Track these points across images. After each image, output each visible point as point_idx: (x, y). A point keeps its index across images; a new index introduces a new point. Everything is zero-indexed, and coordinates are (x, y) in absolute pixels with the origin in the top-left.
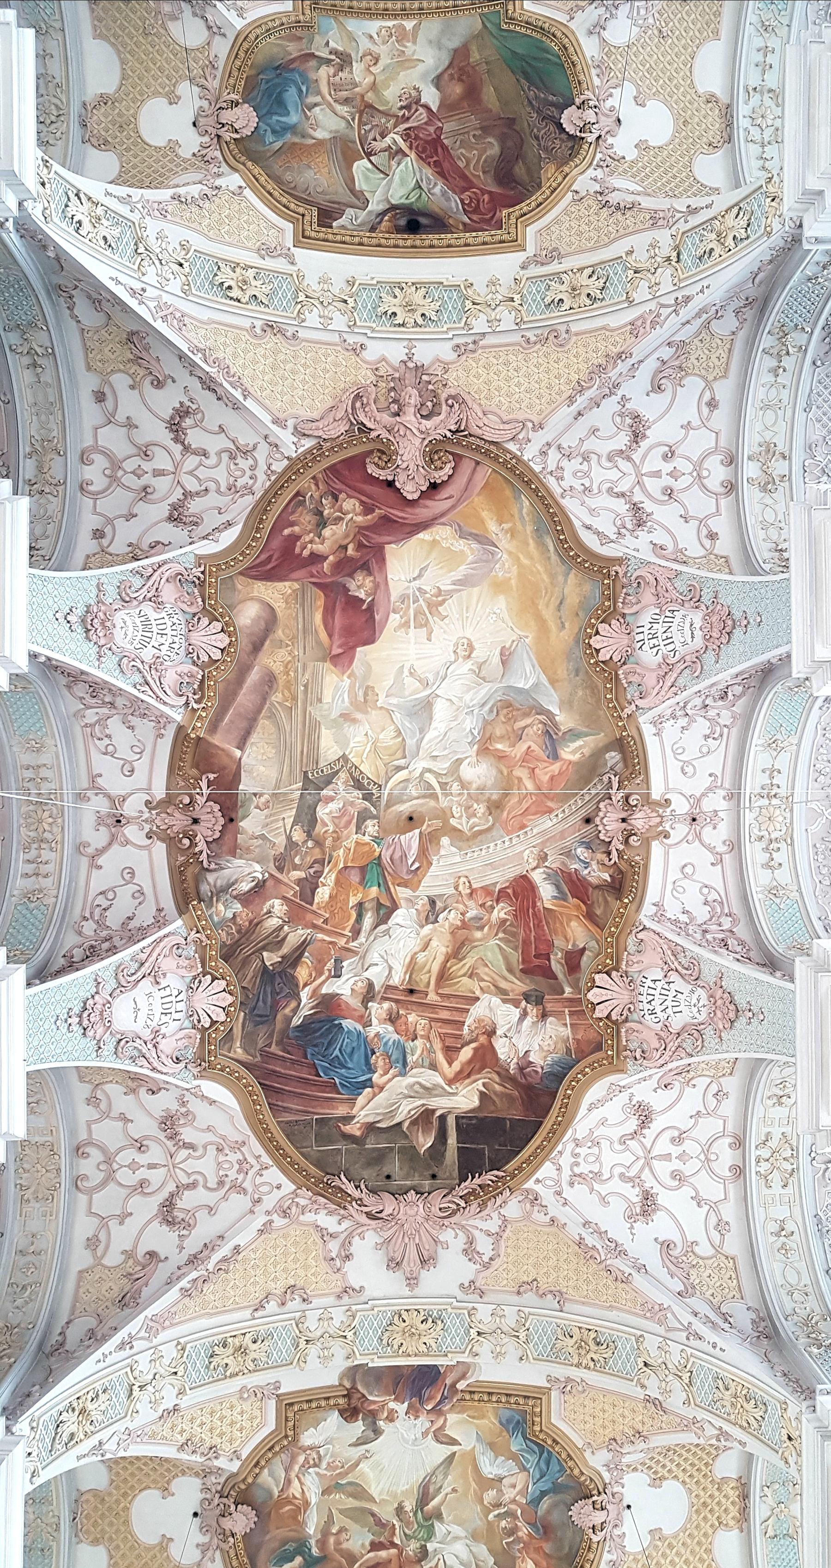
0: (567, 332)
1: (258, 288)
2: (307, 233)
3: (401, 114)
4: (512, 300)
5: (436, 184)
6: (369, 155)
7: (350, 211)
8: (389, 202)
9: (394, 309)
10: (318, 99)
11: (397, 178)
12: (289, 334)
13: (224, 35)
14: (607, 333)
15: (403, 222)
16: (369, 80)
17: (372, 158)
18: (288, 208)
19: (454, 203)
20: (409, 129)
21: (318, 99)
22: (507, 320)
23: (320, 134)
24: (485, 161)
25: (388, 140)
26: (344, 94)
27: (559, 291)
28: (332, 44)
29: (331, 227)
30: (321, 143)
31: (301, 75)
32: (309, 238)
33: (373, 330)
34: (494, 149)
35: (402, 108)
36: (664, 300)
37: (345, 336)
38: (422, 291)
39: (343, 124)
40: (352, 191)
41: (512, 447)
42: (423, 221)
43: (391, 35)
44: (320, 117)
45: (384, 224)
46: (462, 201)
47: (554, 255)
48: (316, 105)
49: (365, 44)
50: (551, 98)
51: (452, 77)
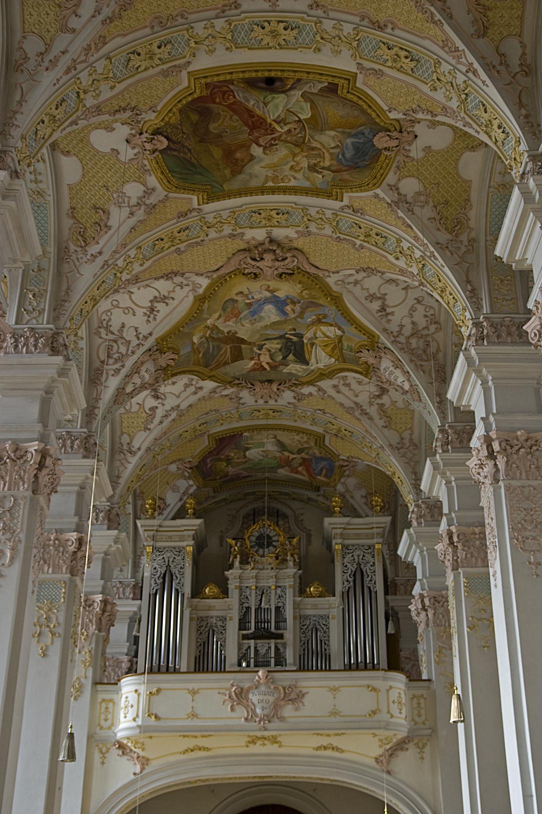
0: (153, 27)
1: (387, 54)
2: (347, 82)
3: (277, 142)
4: (196, 43)
5: (254, 105)
6: (300, 121)
7: (315, 90)
8: (287, 95)
9: (285, 32)
10: (332, 151)
11: (281, 108)
12: (367, 20)
13: (389, 185)
14: (122, 32)
15: (277, 84)
16: (297, 159)
17: (297, 119)
18: (358, 97)
19: (240, 96)
20: (271, 134)
21: (332, 151)
23: (332, 133)
24: (219, 120)
25: (286, 128)
27: (164, 52)
28: (320, 176)
29: (329, 83)
30: (332, 129)
31: (342, 164)
32: (346, 79)
33: (303, 19)
34: (213, 127)
35: (276, 145)
36: (85, 65)
37: (324, 15)
38: (263, 43)
39: (316, 137)
40: (312, 102)
42: (262, 85)
44: (331, 141)
45: (291, 83)
46: (234, 97)
47: (165, 74)
48: (333, 148)
49: (299, 175)
50: (176, 153)
51: (243, 161)
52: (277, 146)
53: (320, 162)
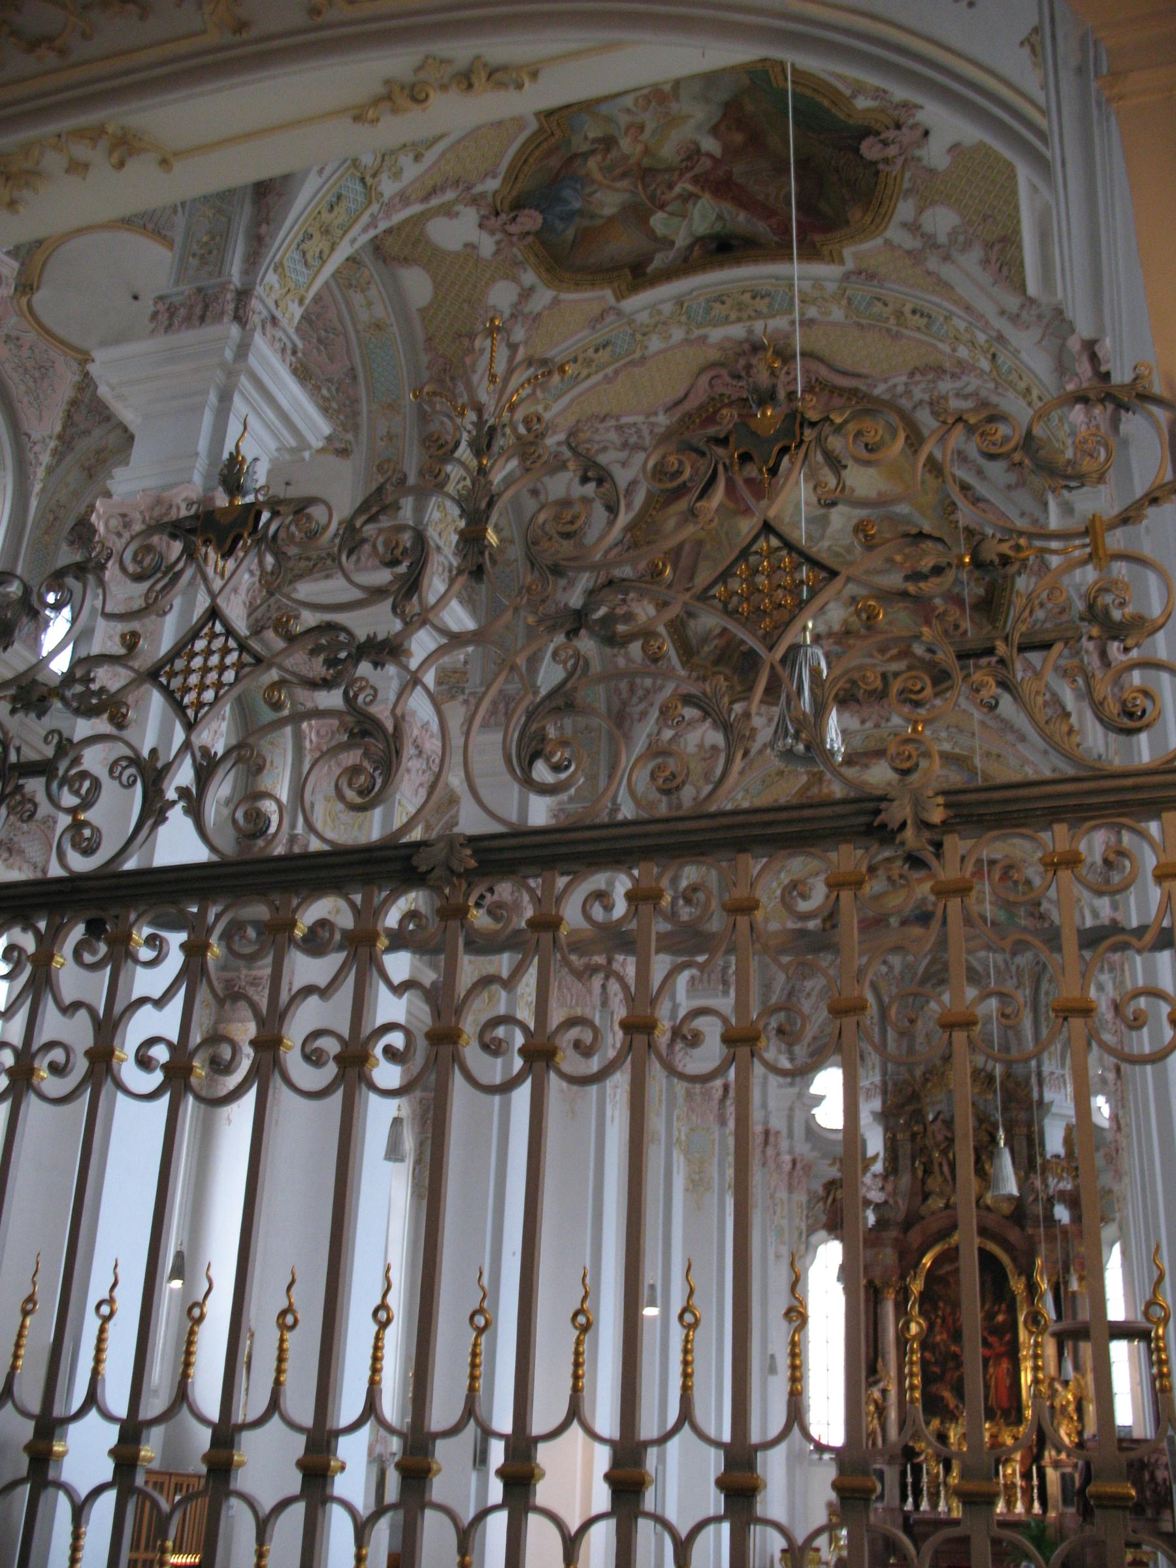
3: (684, 165)
5: (738, 215)
6: (662, 207)
15: (713, 246)
16: (639, 148)
21: (595, 187)
22: (838, 314)
23: (608, 211)
25: (677, 189)
26: (619, 171)
30: (611, 219)
35: (682, 161)
39: (627, 196)
41: (863, 388)
42: (734, 242)
43: (649, 101)
46: (770, 226)
48: (595, 192)
49: (624, 119)
52: (679, 159)
53: (604, 159)
